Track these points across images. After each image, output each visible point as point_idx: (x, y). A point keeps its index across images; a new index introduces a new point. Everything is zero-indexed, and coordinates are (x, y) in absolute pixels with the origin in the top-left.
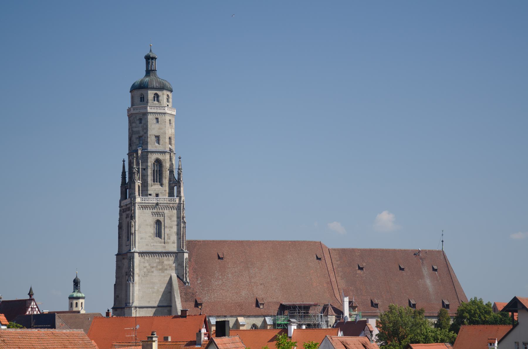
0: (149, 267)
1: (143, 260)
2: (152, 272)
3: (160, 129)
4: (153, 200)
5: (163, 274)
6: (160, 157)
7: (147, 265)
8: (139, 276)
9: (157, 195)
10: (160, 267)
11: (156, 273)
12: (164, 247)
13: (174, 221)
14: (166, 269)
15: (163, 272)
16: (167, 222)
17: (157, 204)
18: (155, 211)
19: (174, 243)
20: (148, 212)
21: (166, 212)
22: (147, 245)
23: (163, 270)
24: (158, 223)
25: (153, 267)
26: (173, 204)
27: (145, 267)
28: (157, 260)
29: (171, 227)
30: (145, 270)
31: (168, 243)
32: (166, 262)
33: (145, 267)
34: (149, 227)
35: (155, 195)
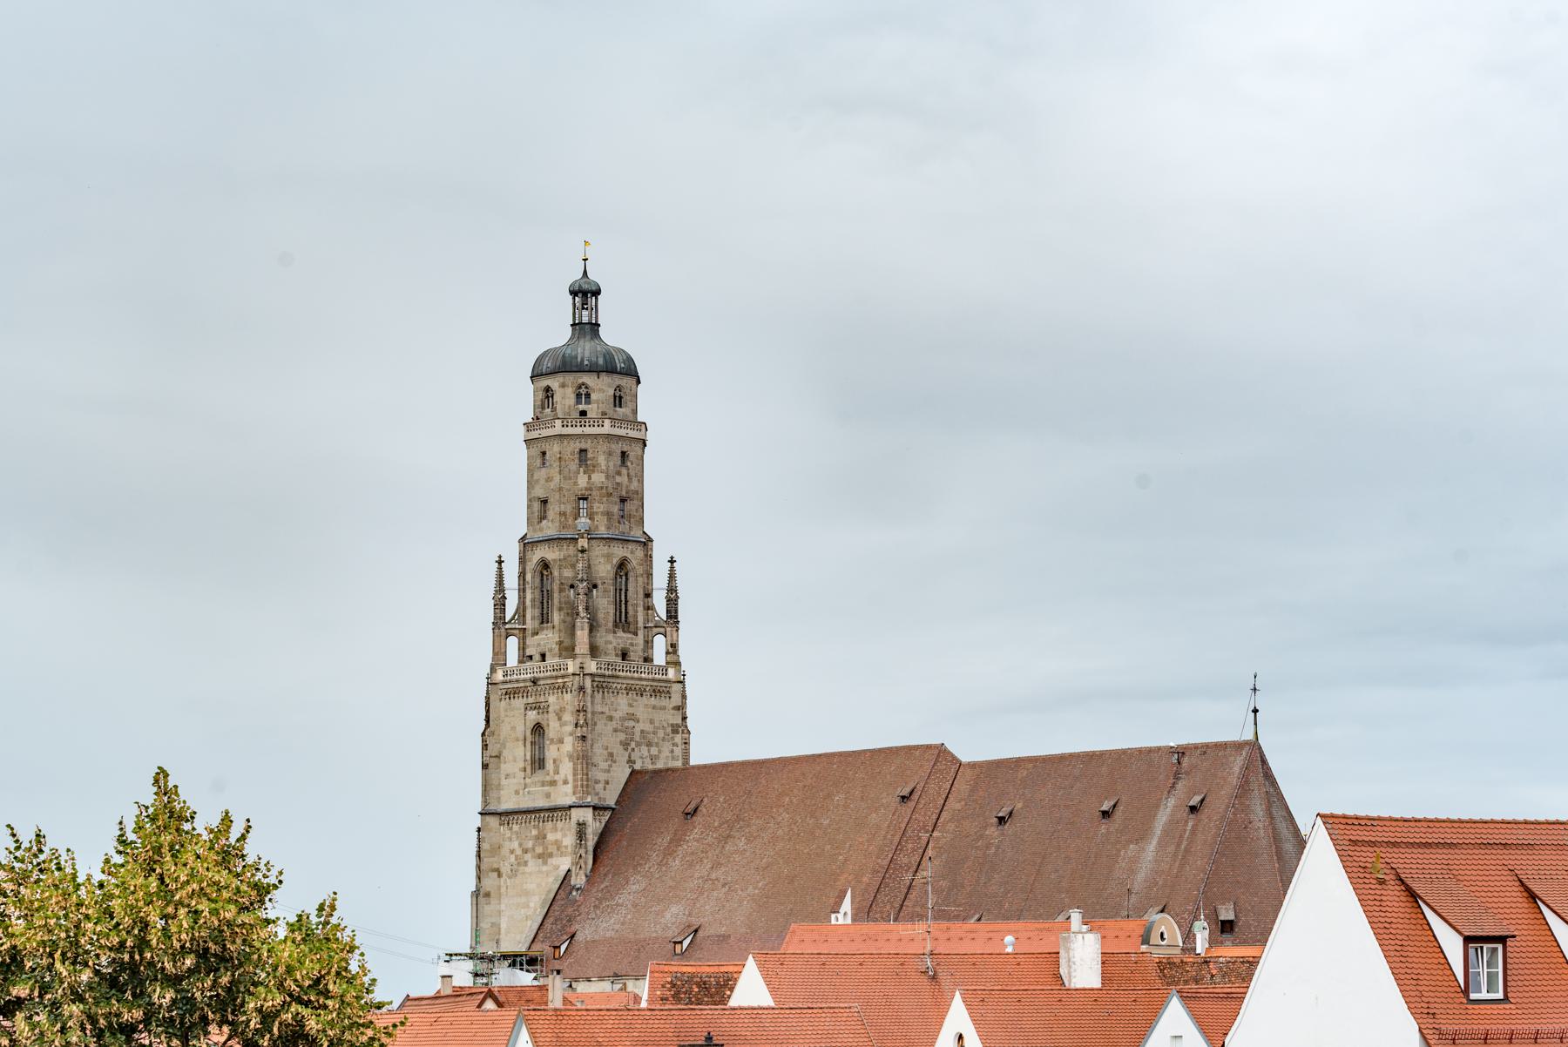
0: (519, 852)
1: (508, 834)
2: (526, 863)
3: (549, 479)
4: (533, 669)
5: (545, 868)
6: (551, 554)
7: (515, 845)
8: (500, 875)
9: (543, 657)
10: (539, 850)
11: (533, 865)
12: (548, 795)
13: (565, 724)
14: (551, 855)
15: (545, 863)
16: (553, 729)
17: (535, 682)
18: (531, 700)
19: (565, 782)
20: (519, 703)
21: (552, 699)
22: (517, 792)
23: (544, 857)
24: (538, 729)
25: (526, 851)
26: (563, 677)
27: (512, 852)
28: (534, 832)
29: (561, 741)
30: (512, 858)
31: (553, 783)
32: (551, 837)
33: (512, 852)
34: (521, 743)
35: (537, 657)
